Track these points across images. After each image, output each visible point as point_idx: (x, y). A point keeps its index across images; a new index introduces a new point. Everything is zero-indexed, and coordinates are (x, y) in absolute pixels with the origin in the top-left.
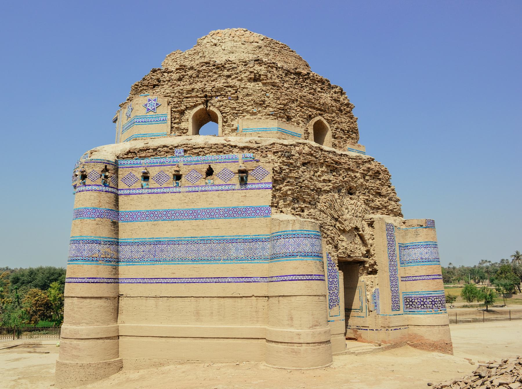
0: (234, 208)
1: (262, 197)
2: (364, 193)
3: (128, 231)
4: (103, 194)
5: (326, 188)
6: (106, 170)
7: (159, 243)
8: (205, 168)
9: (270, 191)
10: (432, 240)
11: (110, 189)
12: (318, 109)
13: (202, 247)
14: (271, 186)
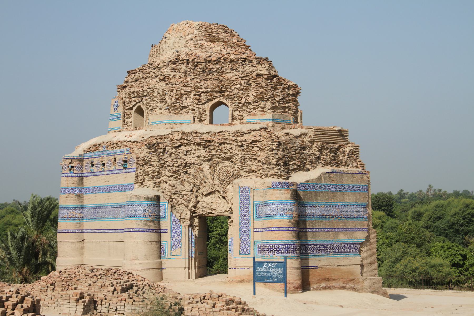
0: (122, 185)
1: (130, 178)
2: (241, 161)
4: (70, 178)
5: (199, 162)
7: (96, 208)
8: (112, 158)
11: (74, 175)
12: (216, 92)
13: (111, 210)
14: (135, 170)
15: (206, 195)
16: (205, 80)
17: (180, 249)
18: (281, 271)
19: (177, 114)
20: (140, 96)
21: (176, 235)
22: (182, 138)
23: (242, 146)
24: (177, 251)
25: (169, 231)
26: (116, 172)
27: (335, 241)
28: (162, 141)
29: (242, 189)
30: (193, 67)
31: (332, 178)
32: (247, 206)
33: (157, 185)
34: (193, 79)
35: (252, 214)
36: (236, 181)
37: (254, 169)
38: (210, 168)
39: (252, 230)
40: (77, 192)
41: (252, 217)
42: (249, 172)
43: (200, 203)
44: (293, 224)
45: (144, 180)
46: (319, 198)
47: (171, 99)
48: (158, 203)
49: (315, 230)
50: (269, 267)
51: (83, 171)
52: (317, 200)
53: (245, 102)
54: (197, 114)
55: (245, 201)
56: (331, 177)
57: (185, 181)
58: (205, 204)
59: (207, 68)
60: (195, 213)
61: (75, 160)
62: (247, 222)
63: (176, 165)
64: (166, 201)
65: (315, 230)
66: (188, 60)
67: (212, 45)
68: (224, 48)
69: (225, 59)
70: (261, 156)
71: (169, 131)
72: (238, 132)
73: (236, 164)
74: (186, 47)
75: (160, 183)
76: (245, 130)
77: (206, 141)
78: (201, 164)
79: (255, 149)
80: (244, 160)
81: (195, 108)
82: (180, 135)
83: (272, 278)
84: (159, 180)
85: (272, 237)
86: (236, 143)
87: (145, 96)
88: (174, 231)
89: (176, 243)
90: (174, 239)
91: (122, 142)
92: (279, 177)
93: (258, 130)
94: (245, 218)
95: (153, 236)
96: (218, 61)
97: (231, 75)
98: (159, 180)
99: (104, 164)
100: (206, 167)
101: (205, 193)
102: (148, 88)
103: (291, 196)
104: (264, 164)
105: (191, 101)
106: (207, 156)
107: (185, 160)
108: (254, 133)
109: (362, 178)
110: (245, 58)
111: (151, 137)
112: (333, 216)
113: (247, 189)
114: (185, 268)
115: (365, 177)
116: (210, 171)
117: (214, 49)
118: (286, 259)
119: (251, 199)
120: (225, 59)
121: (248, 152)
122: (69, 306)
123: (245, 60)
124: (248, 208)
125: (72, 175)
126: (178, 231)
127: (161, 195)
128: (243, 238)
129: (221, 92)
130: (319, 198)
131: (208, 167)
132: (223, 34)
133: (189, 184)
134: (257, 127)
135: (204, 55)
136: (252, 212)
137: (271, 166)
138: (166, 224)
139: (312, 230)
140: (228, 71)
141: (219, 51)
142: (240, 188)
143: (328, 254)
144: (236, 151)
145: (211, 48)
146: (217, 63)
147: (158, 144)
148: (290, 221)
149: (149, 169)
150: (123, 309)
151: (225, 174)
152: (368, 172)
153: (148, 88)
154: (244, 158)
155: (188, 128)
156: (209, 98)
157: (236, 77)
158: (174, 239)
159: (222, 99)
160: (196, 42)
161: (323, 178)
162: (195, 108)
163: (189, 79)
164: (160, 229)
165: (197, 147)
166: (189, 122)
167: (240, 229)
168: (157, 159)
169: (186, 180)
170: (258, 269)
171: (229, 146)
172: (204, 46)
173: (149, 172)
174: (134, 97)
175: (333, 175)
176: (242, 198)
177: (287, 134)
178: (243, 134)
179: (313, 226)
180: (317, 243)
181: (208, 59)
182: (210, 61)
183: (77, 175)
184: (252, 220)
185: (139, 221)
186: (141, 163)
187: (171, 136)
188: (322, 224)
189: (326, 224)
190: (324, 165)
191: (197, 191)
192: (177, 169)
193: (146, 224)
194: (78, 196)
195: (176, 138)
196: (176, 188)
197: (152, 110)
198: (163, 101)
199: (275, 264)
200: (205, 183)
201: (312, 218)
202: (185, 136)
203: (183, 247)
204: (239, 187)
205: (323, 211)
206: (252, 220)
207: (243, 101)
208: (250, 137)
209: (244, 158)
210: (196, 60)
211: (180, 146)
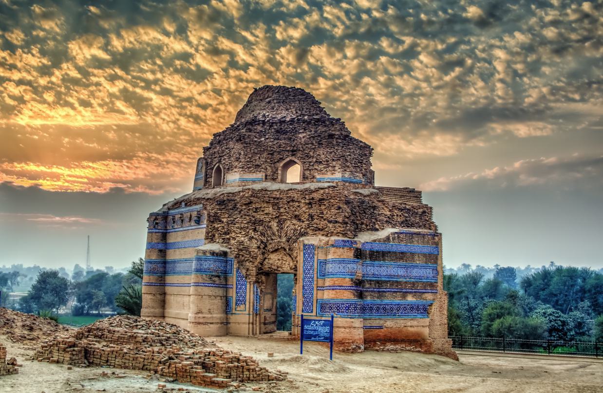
3: (172, 255)
6: (156, 219)
9: (205, 229)
10: (338, 257)
15: (272, 252)
16: (278, 139)
17: (244, 305)
18: (327, 329)
19: (250, 172)
20: (220, 157)
21: (241, 291)
22: (252, 196)
23: (310, 203)
24: (242, 307)
25: (235, 286)
26: (191, 228)
27: (403, 302)
28: (233, 198)
29: (307, 247)
30: (268, 128)
32: (311, 263)
33: (226, 241)
34: (267, 138)
35: (315, 272)
36: (301, 239)
37: (321, 227)
38: (277, 226)
39: (315, 288)
40: (161, 246)
41: (315, 275)
42: (316, 230)
43: (267, 260)
44: (355, 282)
45: (214, 236)
47: (245, 158)
48: (225, 259)
49: (381, 290)
50: (317, 325)
51: (166, 227)
52: (384, 260)
53: (316, 161)
54: (269, 173)
55: (309, 259)
57: (253, 237)
58: (271, 262)
59: (281, 129)
60: (262, 269)
61: (159, 217)
62: (311, 280)
63: (245, 222)
64: (233, 256)
65: (381, 290)
66: (264, 121)
67: (288, 107)
68: (299, 110)
69: (298, 120)
70: (328, 214)
71: (240, 189)
72: (306, 190)
73: (303, 222)
74: (264, 109)
75: (229, 239)
76: (312, 188)
77: (274, 198)
78: (270, 222)
79: (323, 207)
80: (312, 218)
81: (268, 167)
82: (250, 193)
83: (319, 337)
84: (228, 236)
85: (333, 296)
86: (303, 201)
87: (223, 156)
88: (239, 287)
89: (241, 299)
90: (239, 295)
91: (198, 199)
92: (345, 235)
93: (326, 188)
94: (309, 275)
95: (220, 292)
96: (292, 120)
97: (304, 135)
98: (228, 236)
99: (182, 221)
100: (274, 225)
101: (271, 250)
102: (226, 148)
103: (354, 255)
104: (330, 222)
105: (264, 160)
106: (275, 213)
107: (254, 217)
108: (322, 191)
109: (434, 239)
110: (318, 119)
111: (223, 194)
112: (401, 276)
113: (312, 247)
114: (249, 323)
115: (436, 238)
116: (277, 228)
117: (290, 110)
118: (332, 317)
119: (316, 257)
120: (298, 120)
121: (315, 210)
122: (57, 354)
123: (318, 120)
124: (312, 266)
125: (156, 231)
126: (243, 287)
127: (228, 250)
128: (306, 296)
129: (293, 151)
130: (387, 258)
131: (275, 224)
132: (299, 97)
133: (256, 241)
134: (326, 185)
135: (279, 117)
136: (316, 270)
137: (337, 225)
138: (233, 279)
139: (378, 290)
140: (301, 131)
141: (294, 112)
142: (305, 245)
144: (304, 209)
145: (287, 110)
146: (291, 124)
147: (229, 201)
148: (352, 280)
149: (219, 225)
150: (114, 362)
151: (292, 231)
152: (441, 234)
153: (226, 148)
154: (311, 217)
155: (257, 186)
156: (281, 157)
157: (308, 137)
158: (239, 295)
159: (293, 158)
160: (273, 105)
161: (391, 238)
162: (268, 167)
163: (263, 139)
164: (226, 285)
165: (265, 205)
166: (260, 181)
167: (303, 286)
168: (227, 216)
169: (254, 236)
170: (306, 327)
171: (297, 204)
172: (281, 108)
173: (218, 228)
174: (215, 158)
175: (401, 236)
176: (307, 255)
177: (356, 193)
178: (312, 192)
181: (282, 120)
182: (284, 122)
183: (160, 231)
184: (315, 278)
185: (204, 275)
186: (212, 219)
187: (241, 194)
188: (388, 285)
189: (393, 285)
190: (394, 226)
191: (264, 248)
192: (246, 225)
193: (210, 279)
194: (160, 251)
195: (246, 195)
196: (243, 245)
197: (229, 168)
198: (238, 159)
199: (322, 323)
200: (272, 239)
202: (255, 194)
203: (247, 303)
204: (304, 244)
205: (390, 271)
206: (315, 278)
207: (314, 160)
208: (316, 196)
209: (311, 217)
210: (271, 121)
211: (251, 203)
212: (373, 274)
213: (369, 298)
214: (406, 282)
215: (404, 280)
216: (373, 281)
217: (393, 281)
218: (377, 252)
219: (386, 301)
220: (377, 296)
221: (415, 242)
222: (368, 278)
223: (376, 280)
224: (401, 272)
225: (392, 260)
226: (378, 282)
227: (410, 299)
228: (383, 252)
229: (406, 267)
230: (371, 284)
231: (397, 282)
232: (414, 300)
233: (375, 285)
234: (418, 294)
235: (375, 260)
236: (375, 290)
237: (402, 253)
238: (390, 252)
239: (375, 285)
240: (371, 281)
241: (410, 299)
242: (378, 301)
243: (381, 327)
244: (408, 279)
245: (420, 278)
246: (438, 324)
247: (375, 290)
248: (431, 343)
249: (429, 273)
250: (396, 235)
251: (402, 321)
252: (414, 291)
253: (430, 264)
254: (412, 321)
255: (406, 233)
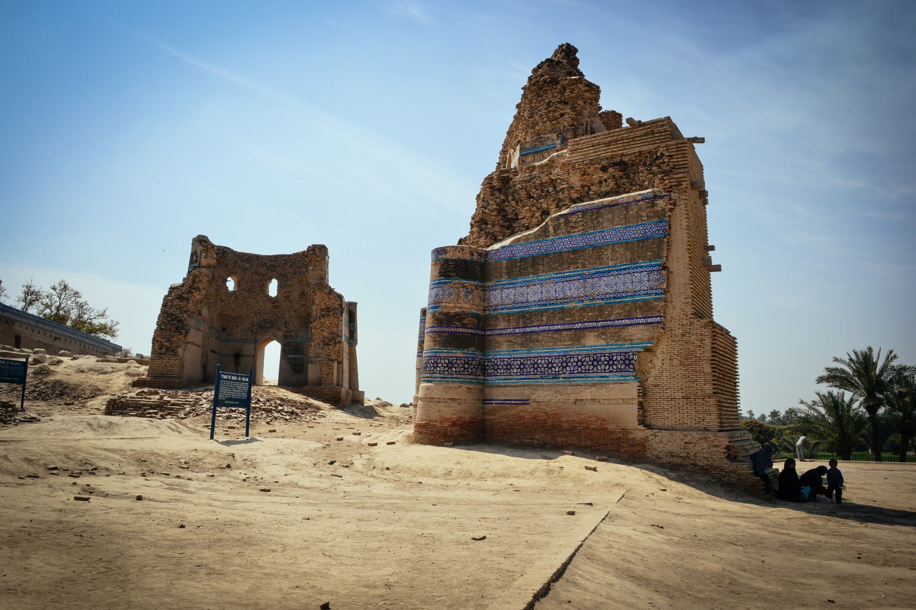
27: (574, 350)
31: (571, 224)
46: (541, 268)
49: (528, 330)
52: (535, 273)
56: (571, 221)
65: (528, 330)
112: (572, 299)
130: (541, 268)
139: (522, 330)
143: (556, 376)
161: (551, 229)
179: (524, 323)
180: (533, 355)
188: (544, 318)
189: (554, 316)
201: (525, 307)
205: (548, 291)
212: (515, 302)
213: (504, 347)
214: (583, 309)
215: (580, 305)
216: (514, 314)
217: (554, 309)
218: (523, 260)
219: (538, 351)
220: (520, 342)
221: (606, 224)
222: (505, 311)
223: (518, 313)
224: (572, 289)
225: (553, 270)
226: (523, 315)
227: (592, 342)
228: (534, 257)
229: (583, 277)
230: (509, 321)
231: (563, 310)
232: (602, 342)
233: (518, 323)
234: (613, 330)
235: (517, 277)
236: (517, 331)
237: (575, 251)
238: (547, 255)
239: (518, 323)
240: (509, 315)
241: (592, 342)
242: (522, 353)
243: (525, 402)
244: (588, 302)
245: (617, 295)
246: (679, 395)
247: (517, 331)
248: (646, 439)
249: (640, 282)
250: (562, 220)
251: (570, 390)
252: (600, 324)
253: (641, 263)
254: (593, 389)
255: (584, 212)
